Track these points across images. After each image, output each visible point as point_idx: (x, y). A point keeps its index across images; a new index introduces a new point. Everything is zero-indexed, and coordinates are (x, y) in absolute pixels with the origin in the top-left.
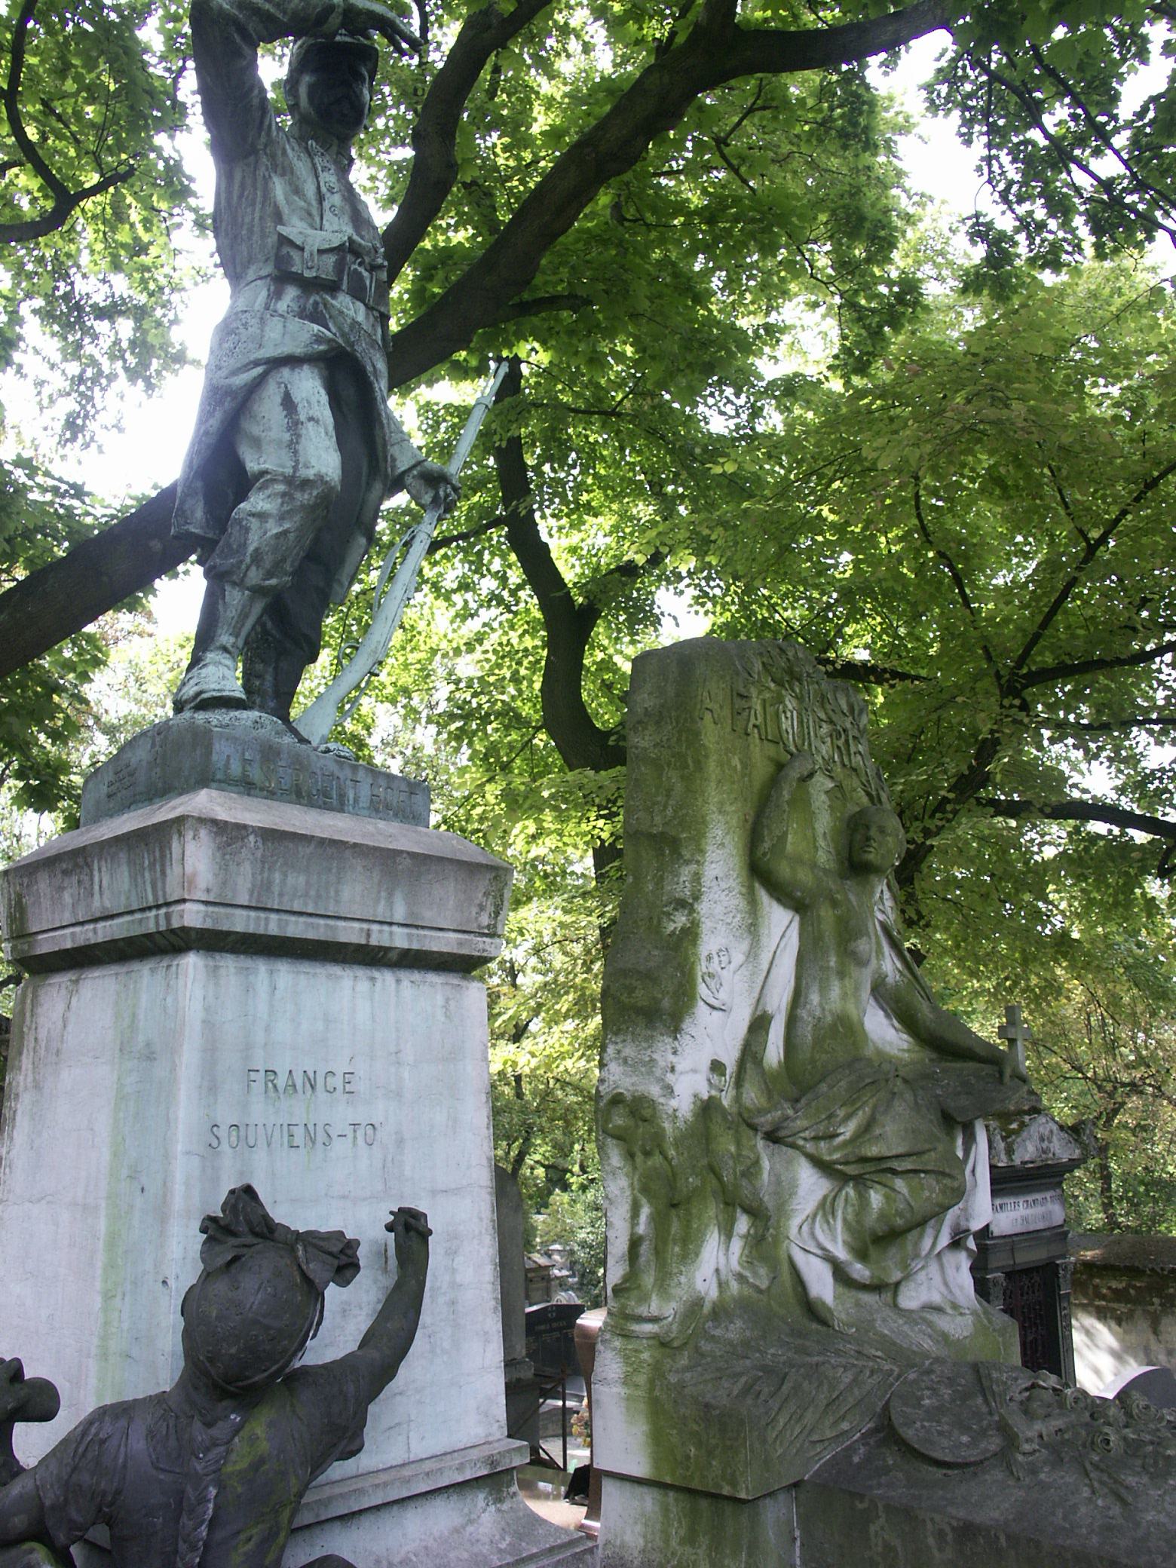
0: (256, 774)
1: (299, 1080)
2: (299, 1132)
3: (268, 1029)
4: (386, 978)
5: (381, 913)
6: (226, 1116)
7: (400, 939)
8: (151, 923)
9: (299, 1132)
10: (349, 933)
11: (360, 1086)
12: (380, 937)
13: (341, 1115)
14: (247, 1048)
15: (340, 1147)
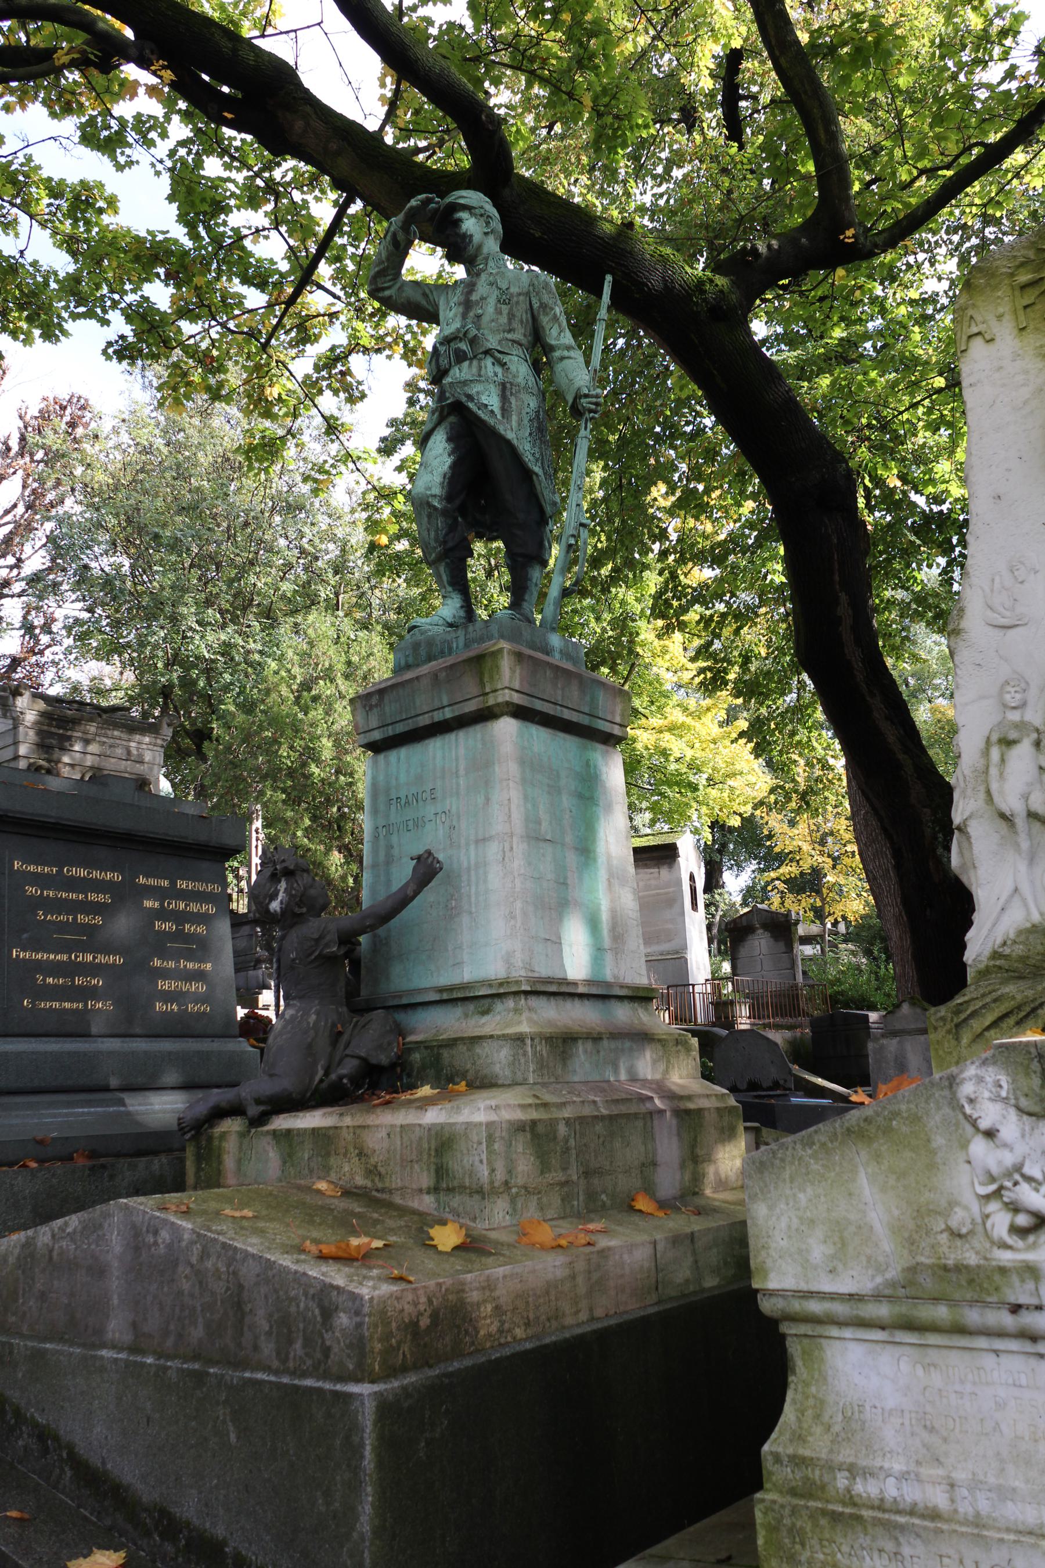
0: (411, 660)
1: (410, 798)
2: (411, 823)
3: (397, 779)
4: (452, 737)
5: (437, 704)
6: (382, 822)
7: (448, 714)
8: (585, 720)
9: (411, 823)
10: (424, 721)
11: (438, 794)
12: (438, 716)
13: (430, 810)
14: (388, 790)
15: (429, 827)
